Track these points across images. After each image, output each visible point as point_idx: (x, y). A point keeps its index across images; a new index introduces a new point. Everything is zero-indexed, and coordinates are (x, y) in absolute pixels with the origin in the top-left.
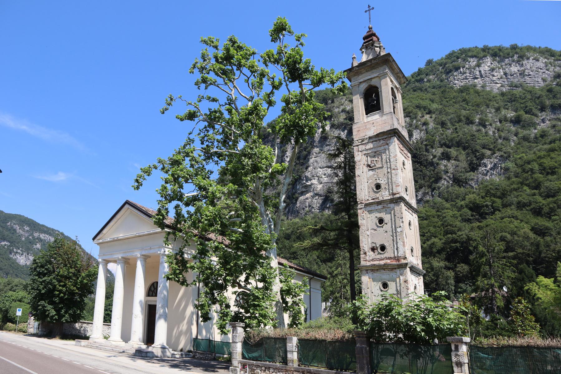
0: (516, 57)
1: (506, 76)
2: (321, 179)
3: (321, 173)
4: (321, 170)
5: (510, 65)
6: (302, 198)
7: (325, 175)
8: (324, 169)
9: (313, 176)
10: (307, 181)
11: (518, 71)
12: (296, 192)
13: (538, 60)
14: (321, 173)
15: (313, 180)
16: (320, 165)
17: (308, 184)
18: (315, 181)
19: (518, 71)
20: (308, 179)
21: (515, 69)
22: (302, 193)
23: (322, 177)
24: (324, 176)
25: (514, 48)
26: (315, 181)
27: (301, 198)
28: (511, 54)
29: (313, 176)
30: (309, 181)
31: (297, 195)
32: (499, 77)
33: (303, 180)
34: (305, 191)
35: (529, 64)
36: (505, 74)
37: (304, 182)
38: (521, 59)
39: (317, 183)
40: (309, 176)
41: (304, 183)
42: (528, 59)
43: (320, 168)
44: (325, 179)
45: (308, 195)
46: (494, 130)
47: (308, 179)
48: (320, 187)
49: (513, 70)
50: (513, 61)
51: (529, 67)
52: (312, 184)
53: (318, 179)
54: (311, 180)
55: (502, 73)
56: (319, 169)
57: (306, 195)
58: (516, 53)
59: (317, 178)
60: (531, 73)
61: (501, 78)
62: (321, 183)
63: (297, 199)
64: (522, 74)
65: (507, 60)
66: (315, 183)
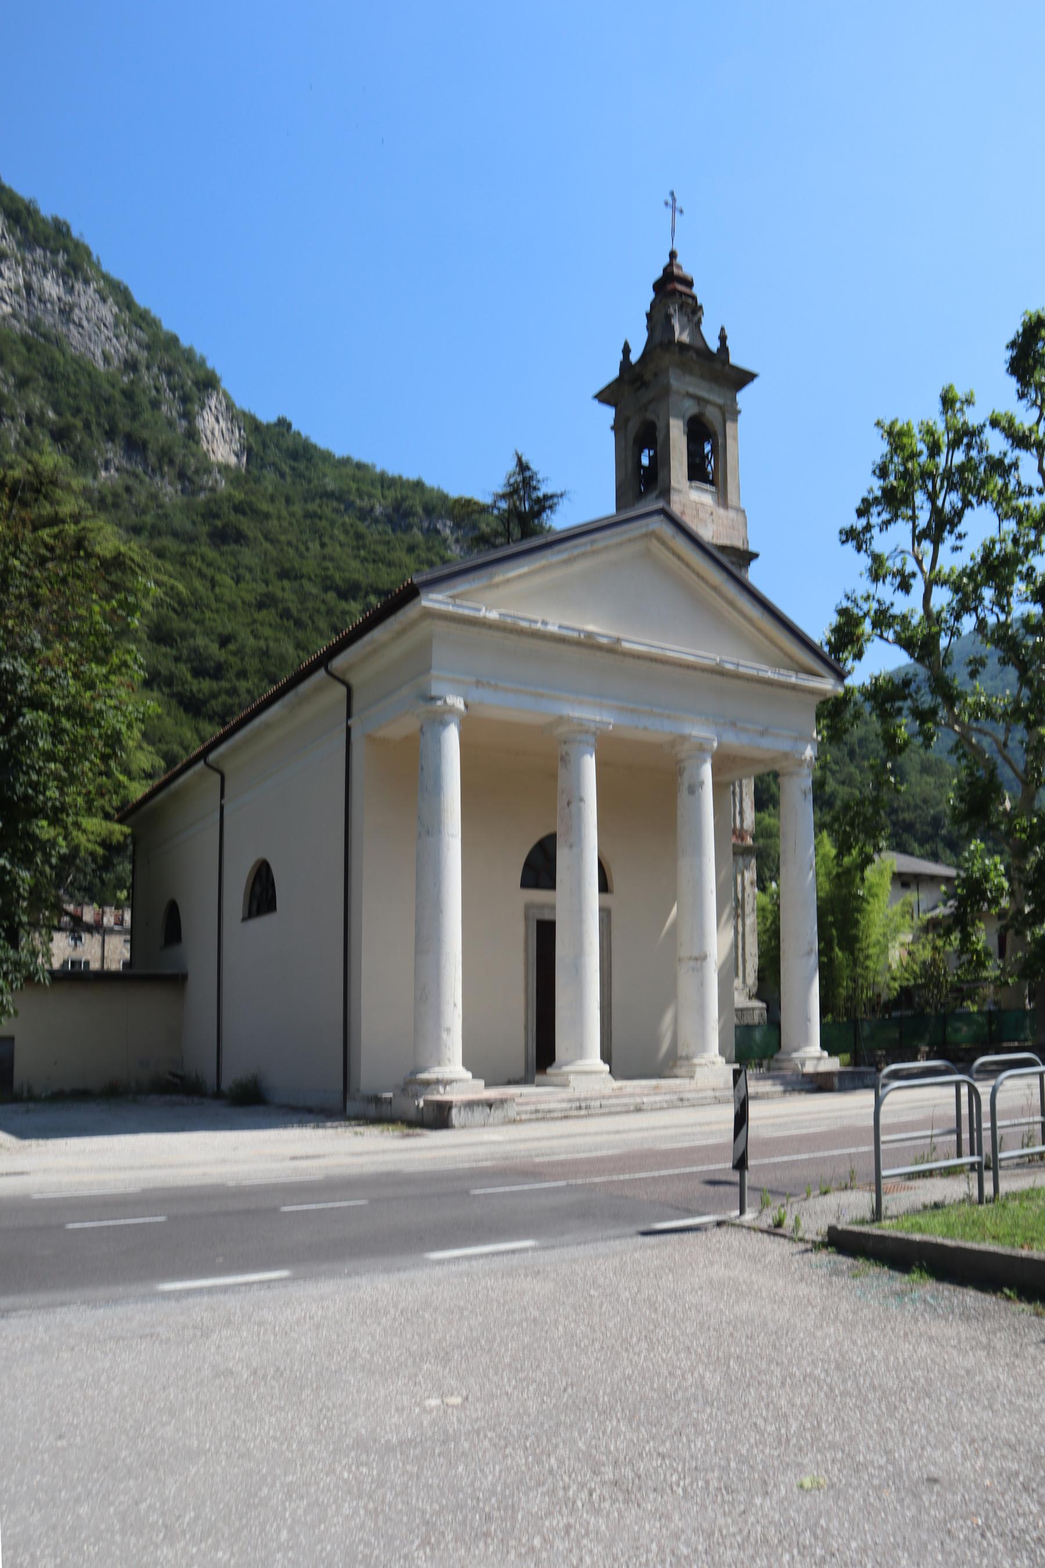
0: (61, 259)
1: (28, 294)
5: (45, 272)
11: (59, 299)
13: (104, 300)
19: (59, 299)
21: (51, 287)
25: (61, 229)
28: (52, 243)
32: (12, 285)
35: (86, 296)
36: (29, 287)
38: (72, 274)
42: (86, 282)
46: (18, 437)
49: (47, 289)
50: (55, 266)
51: (83, 306)
55: (21, 282)
58: (66, 250)
60: (85, 323)
61: (17, 292)
64: (66, 313)
65: (39, 252)
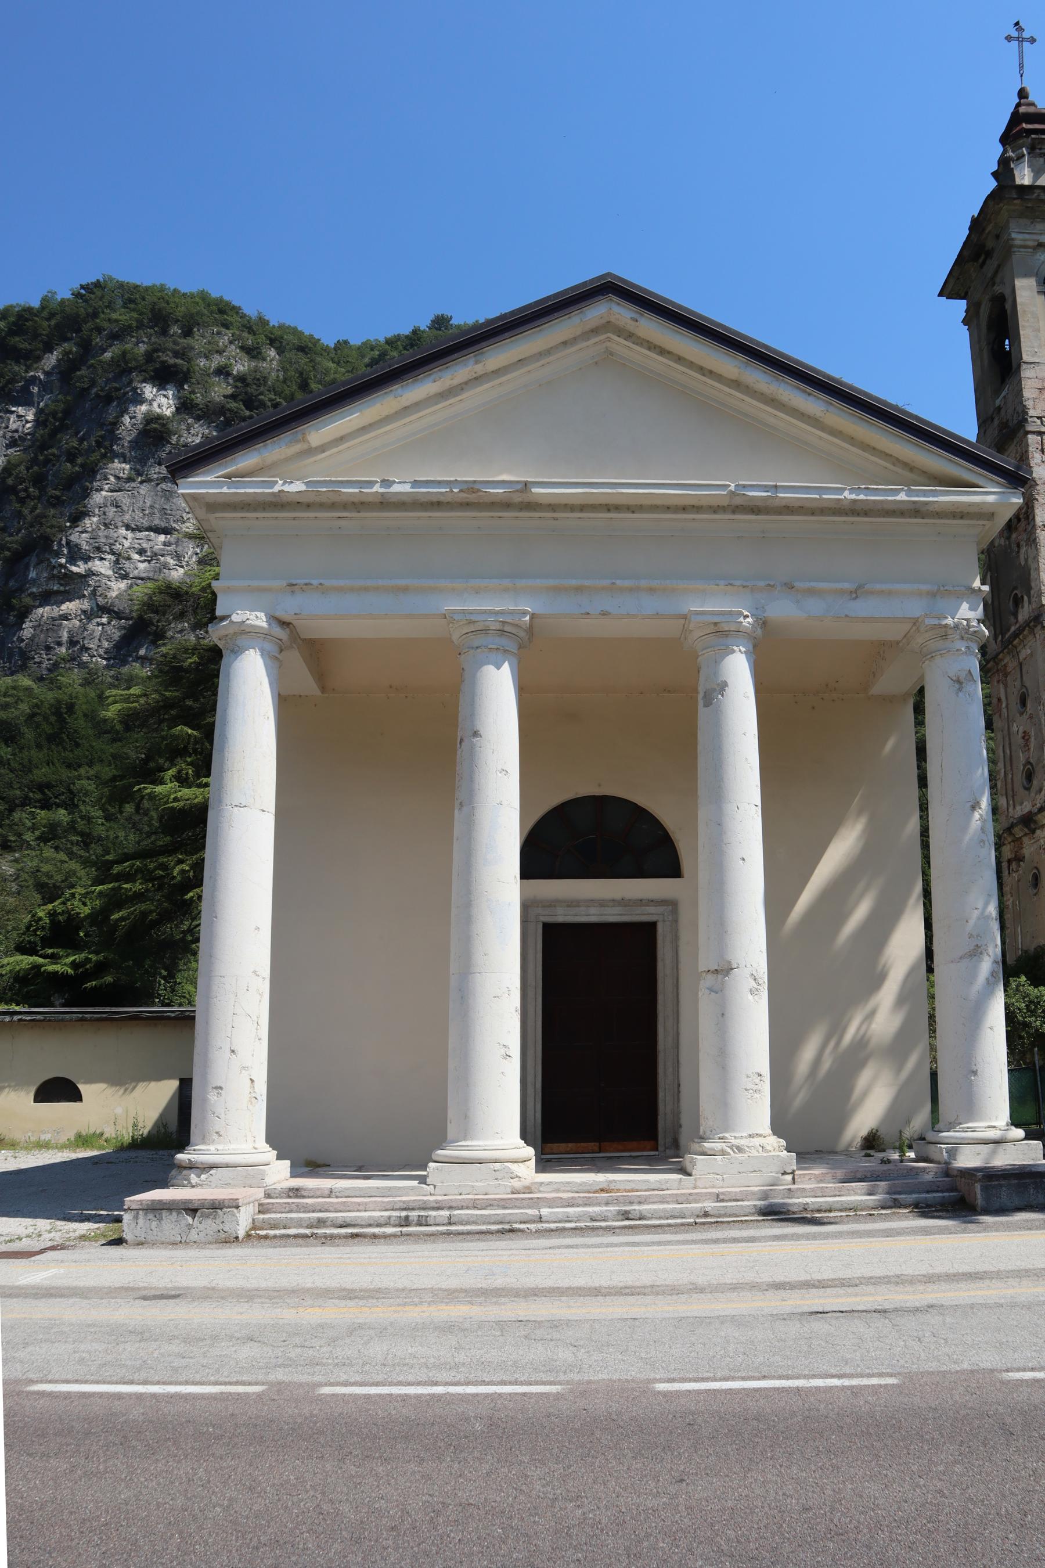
2: (127, 565)
3: (127, 544)
4: (130, 535)
6: (45, 612)
7: (141, 552)
8: (139, 535)
9: (98, 549)
10: (72, 559)
12: (21, 590)
14: (127, 544)
15: (97, 562)
16: (127, 518)
17: (74, 569)
18: (102, 567)
20: (76, 554)
22: (47, 598)
23: (129, 558)
24: (136, 557)
26: (102, 567)
27: (40, 610)
29: (98, 549)
30: (80, 563)
31: (28, 600)
33: (58, 554)
34: (58, 592)
37: (63, 561)
39: (110, 573)
40: (85, 546)
41: (61, 566)
43: (128, 527)
44: (142, 566)
45: (70, 607)
47: (76, 554)
48: (117, 587)
52: (91, 573)
53: (117, 562)
54: (87, 559)
56: (123, 531)
57: (64, 607)
59: (113, 558)
62: (125, 577)
63: (24, 614)
66: (103, 571)
